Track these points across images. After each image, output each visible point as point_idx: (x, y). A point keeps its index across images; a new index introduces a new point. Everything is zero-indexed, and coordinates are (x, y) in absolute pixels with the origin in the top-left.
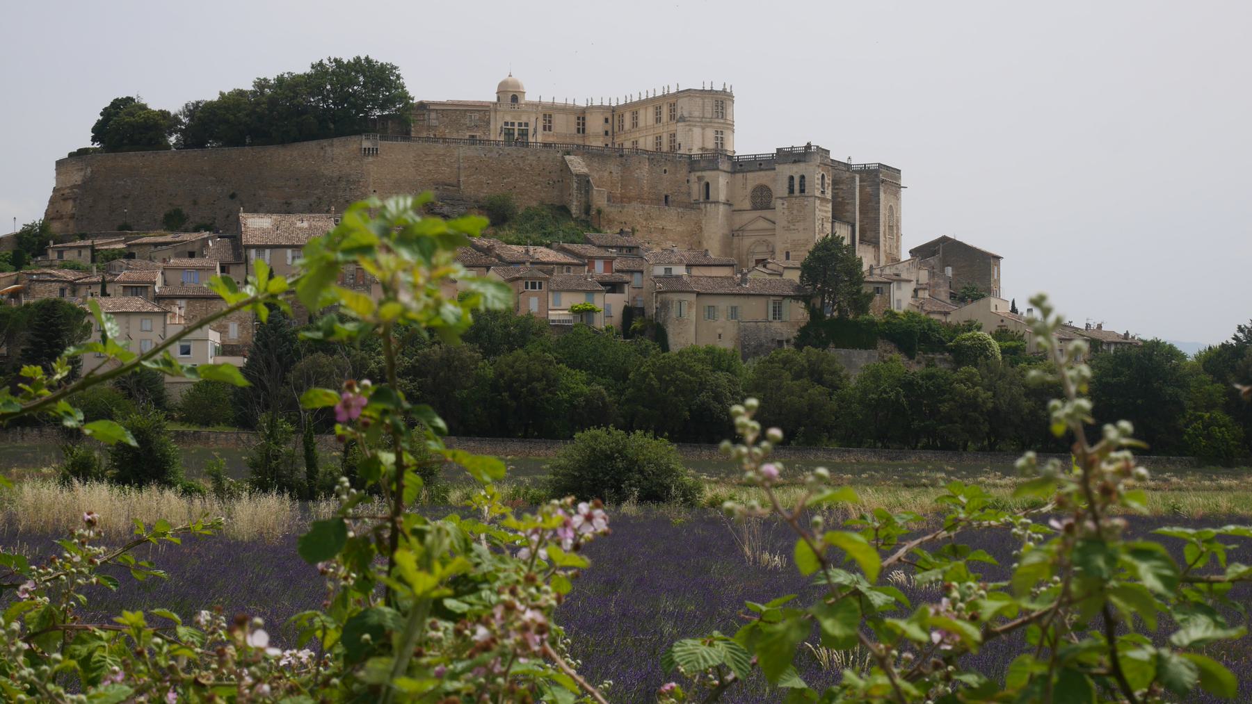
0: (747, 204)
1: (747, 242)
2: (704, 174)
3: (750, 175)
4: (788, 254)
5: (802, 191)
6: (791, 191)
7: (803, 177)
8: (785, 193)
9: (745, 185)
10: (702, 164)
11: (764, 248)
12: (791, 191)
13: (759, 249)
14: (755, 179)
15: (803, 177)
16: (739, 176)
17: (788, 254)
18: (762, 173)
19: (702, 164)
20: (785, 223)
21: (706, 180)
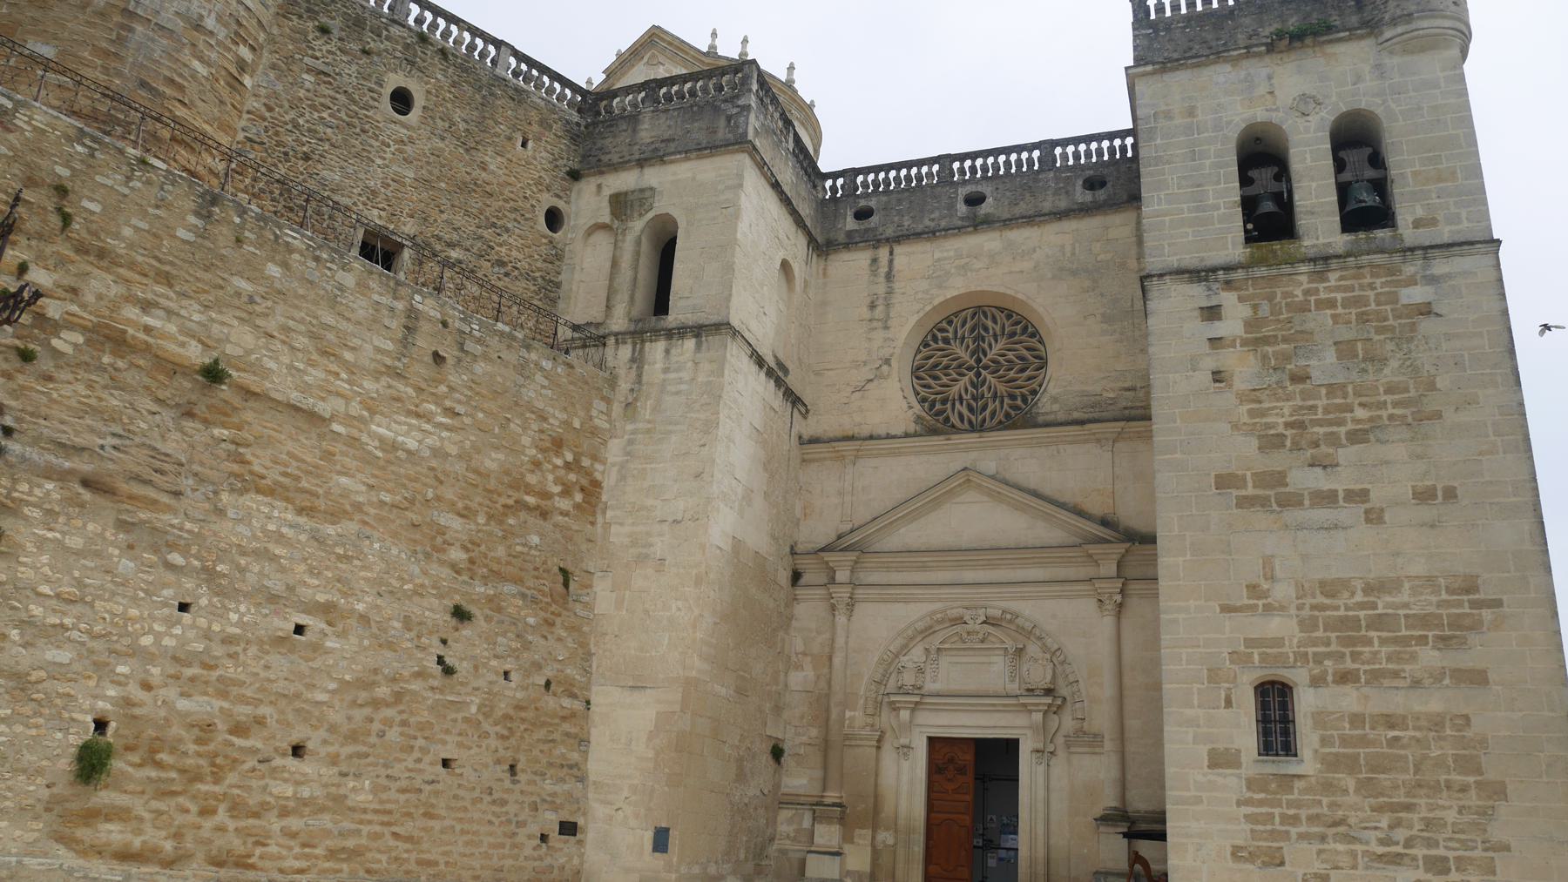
0: (893, 403)
1: (878, 625)
2: (653, 177)
3: (911, 259)
5: (1366, 210)
6: (1270, 221)
8: (1226, 237)
9: (879, 308)
11: (993, 672)
13: (951, 674)
14: (939, 272)
15: (1356, 141)
16: (854, 263)
18: (988, 241)
20: (1243, 453)
21: (661, 206)
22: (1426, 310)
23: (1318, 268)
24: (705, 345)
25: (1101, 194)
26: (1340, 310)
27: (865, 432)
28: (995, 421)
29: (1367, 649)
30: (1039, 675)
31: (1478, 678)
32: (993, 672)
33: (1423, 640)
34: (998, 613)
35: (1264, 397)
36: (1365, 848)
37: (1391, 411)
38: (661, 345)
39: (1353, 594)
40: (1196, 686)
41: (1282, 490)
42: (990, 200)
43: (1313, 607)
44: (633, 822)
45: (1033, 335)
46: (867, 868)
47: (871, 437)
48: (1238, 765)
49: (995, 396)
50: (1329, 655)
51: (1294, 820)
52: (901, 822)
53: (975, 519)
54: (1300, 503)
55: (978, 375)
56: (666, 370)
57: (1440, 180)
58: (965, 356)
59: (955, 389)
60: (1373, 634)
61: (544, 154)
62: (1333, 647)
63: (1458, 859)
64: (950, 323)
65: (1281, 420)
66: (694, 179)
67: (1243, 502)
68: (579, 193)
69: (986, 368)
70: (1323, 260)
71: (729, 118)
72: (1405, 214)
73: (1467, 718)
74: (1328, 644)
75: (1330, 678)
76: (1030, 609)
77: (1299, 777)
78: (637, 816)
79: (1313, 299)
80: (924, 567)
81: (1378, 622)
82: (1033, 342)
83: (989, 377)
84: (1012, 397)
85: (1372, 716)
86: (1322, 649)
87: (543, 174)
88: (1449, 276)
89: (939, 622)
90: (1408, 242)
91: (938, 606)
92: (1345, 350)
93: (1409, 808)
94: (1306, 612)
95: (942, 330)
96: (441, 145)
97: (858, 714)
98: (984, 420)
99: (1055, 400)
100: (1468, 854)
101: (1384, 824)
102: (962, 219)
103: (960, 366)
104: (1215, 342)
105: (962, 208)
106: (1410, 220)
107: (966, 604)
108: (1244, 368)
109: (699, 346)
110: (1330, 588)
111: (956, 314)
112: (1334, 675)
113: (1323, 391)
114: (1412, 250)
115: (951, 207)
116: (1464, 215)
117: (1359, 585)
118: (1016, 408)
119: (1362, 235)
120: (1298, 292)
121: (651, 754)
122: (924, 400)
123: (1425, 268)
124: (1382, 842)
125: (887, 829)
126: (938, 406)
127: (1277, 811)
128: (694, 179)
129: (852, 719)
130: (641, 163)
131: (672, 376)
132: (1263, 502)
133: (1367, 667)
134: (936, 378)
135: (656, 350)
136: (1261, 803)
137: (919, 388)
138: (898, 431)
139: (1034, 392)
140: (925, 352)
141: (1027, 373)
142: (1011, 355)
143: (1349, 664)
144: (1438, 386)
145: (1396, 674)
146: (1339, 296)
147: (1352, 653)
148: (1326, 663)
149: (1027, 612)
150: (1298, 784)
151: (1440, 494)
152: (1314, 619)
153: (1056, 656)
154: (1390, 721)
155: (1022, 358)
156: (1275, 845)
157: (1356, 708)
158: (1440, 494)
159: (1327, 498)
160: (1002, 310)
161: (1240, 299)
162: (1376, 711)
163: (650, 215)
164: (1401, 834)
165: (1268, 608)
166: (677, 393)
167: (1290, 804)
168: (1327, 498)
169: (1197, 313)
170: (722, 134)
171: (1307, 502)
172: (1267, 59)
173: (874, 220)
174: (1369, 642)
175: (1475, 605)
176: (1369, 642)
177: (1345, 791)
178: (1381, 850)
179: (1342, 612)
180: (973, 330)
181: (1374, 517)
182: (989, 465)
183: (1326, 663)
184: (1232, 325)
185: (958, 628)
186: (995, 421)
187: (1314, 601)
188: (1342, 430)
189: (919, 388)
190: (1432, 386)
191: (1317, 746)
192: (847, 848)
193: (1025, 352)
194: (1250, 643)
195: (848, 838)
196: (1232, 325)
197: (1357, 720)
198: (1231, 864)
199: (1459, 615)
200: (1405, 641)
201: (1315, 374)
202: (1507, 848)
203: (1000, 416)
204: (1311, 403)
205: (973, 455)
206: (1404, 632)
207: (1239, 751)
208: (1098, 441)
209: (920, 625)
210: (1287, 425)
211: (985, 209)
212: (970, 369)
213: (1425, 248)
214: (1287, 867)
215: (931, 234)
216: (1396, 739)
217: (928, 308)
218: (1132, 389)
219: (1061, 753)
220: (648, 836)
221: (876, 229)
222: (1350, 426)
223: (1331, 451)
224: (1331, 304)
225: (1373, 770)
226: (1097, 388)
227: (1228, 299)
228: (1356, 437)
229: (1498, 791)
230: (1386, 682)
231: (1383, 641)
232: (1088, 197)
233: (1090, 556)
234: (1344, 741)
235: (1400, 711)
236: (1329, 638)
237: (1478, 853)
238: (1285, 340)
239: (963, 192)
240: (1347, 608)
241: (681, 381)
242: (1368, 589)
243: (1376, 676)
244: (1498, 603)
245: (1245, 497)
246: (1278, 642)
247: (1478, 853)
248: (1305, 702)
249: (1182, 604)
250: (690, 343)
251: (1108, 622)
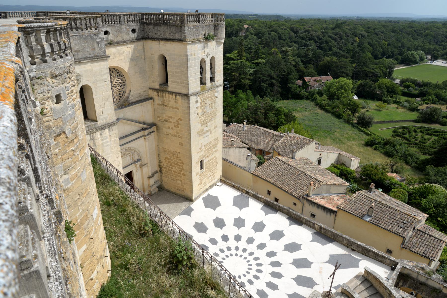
24: (111, 129)
38: (98, 133)
56: (102, 140)
71: (98, 43)
82: (122, 78)
99: (132, 96)
109: (109, 130)
128: (92, 70)
141: (122, 87)
154: (211, 160)
160: (114, 69)
166: (108, 145)
184: (199, 104)
193: (121, 81)
196: (199, 104)
211: (111, 37)
219: (139, 169)
226: (139, 92)
239: (104, 29)
241: (107, 142)
250: (107, 130)
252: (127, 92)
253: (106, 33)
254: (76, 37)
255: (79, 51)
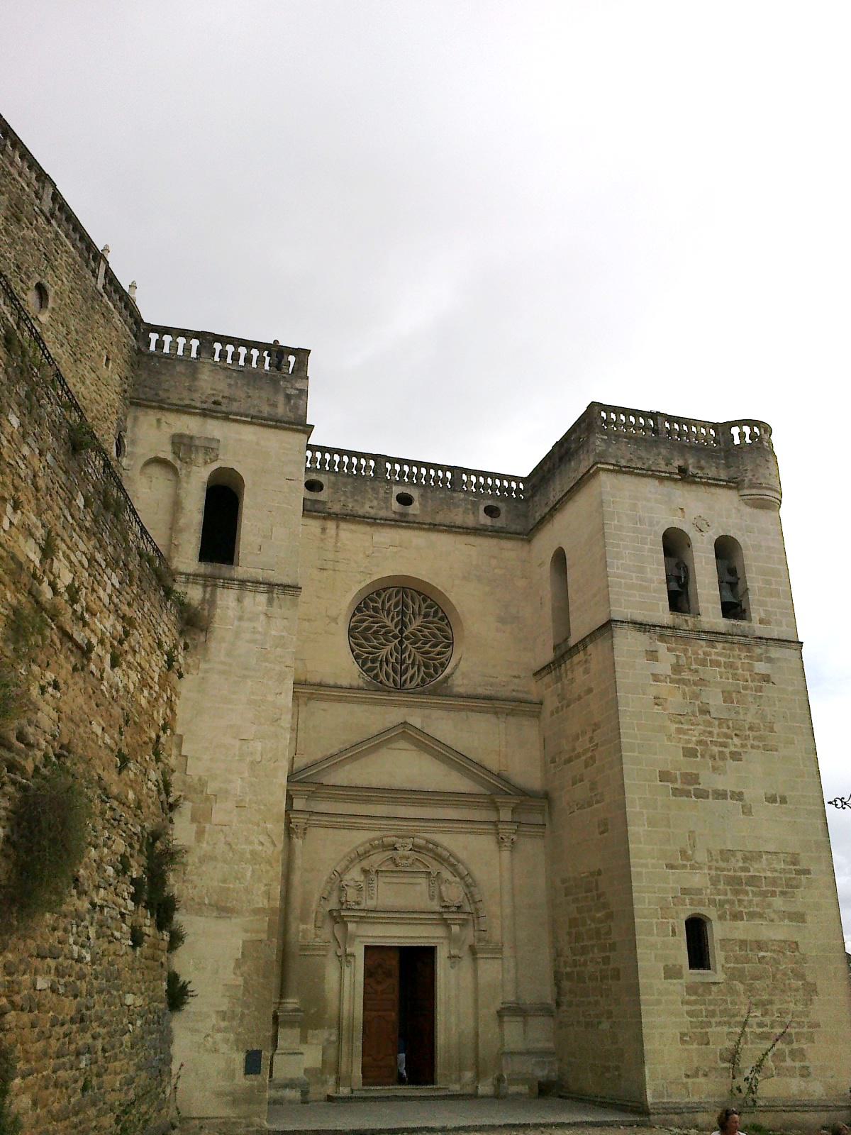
2: (215, 429)
4: (696, 929)
6: (680, 598)
7: (725, 549)
10: (209, 383)
12: (680, 598)
13: (386, 894)
17: (696, 929)
18: (417, 539)
19: (209, 383)
21: (227, 460)
22: (766, 678)
23: (713, 638)
24: (276, 602)
25: (500, 522)
26: (723, 669)
27: (316, 679)
28: (414, 683)
29: (746, 898)
30: (454, 893)
31: (799, 917)
32: (416, 894)
33: (773, 894)
34: (422, 842)
35: (683, 721)
36: (751, 1030)
37: (752, 742)
39: (738, 861)
40: (655, 920)
41: (697, 786)
42: (416, 504)
43: (717, 869)
44: (224, 1048)
45: (442, 619)
46: (319, 1065)
47: (320, 685)
48: (681, 978)
49: (413, 664)
50: (728, 901)
51: (713, 1014)
52: (345, 1023)
53: (404, 767)
54: (708, 797)
55: (401, 643)
56: (240, 619)
57: (771, 595)
58: (392, 626)
59: (383, 653)
60: (749, 888)
61: (117, 378)
62: (730, 896)
63: (796, 1033)
64: (379, 595)
65: (694, 739)
66: (258, 444)
67: (676, 792)
68: (136, 419)
69: (407, 638)
70: (713, 636)
71: (288, 397)
72: (756, 612)
73: (796, 943)
74: (726, 895)
75: (728, 917)
76: (451, 842)
77: (714, 983)
78: (227, 1041)
79: (708, 658)
80: (367, 801)
81: (753, 880)
83: (410, 646)
84: (427, 666)
85: (751, 941)
86: (722, 897)
87: (115, 396)
88: (778, 659)
89: (374, 847)
90: (758, 634)
91: (378, 834)
92: (727, 698)
93: (771, 1002)
94: (713, 872)
95: (373, 600)
96: (60, 351)
97: (310, 927)
98: (405, 681)
100: (801, 1030)
101: (758, 1014)
102: (395, 512)
103: (386, 633)
104: (656, 678)
105: (395, 505)
106: (758, 618)
107: (400, 833)
108: (675, 698)
109: (270, 602)
110: (726, 855)
111: (385, 590)
112: (730, 913)
113: (716, 723)
114: (760, 638)
115: (387, 500)
116: (784, 623)
117: (739, 855)
118: (431, 676)
119: (733, 622)
120: (700, 652)
121: (240, 981)
122: (357, 657)
123: (767, 651)
124: (760, 1025)
125: (330, 1027)
126: (369, 664)
127: (703, 1007)
128: (258, 444)
129: (305, 932)
130: (205, 414)
131: (246, 624)
132: (687, 794)
133: (746, 911)
134: (367, 639)
135: (227, 600)
136: (695, 1002)
137: (352, 644)
138: (345, 683)
139: (443, 666)
140: (359, 616)
141: (438, 649)
142: (426, 632)
143: (737, 908)
144: (775, 730)
145: (761, 916)
146: (722, 659)
147: (739, 900)
148: (727, 906)
149: (445, 844)
150: (714, 988)
151: (778, 799)
152: (718, 876)
153: (469, 884)
154: (760, 945)
155: (434, 635)
156: (703, 1031)
157: (742, 937)
158: (778, 799)
159: (721, 795)
160: (419, 593)
161: (669, 649)
162: (753, 939)
163: (215, 466)
164: (767, 1020)
165: (692, 867)
167: (711, 1003)
168: (721, 795)
169: (644, 654)
170: (281, 410)
171: (711, 797)
172: (680, 484)
173: (323, 496)
174: (746, 893)
175: (799, 872)
176: (746, 893)
177: (738, 995)
178: (759, 1030)
179: (731, 873)
180: (396, 605)
181: (747, 811)
182: (416, 719)
183: (727, 906)
184: (664, 666)
185: (389, 854)
186: (414, 683)
187: (717, 865)
188: (727, 750)
189: (352, 644)
190: (772, 730)
191: (723, 962)
192: (303, 1048)
193: (436, 631)
194: (685, 891)
195: (304, 1040)
197: (743, 944)
198: (680, 1046)
199: (790, 878)
200: (764, 894)
201: (712, 710)
202: (818, 1025)
203: (417, 680)
204: (709, 729)
205: (404, 710)
206: (765, 889)
207: (681, 966)
208: (496, 713)
209: (361, 850)
210: (700, 742)
211: (414, 509)
212: (395, 637)
213: (767, 639)
214: (711, 1046)
215: (372, 521)
216: (763, 957)
217: (369, 581)
218: (519, 677)
220: (239, 1059)
221: (324, 503)
222: (733, 749)
223: (721, 763)
224: (718, 664)
225: (752, 979)
227: (662, 647)
228: (736, 756)
229: (811, 989)
230: (758, 921)
231: (755, 894)
232: (485, 520)
233: (495, 803)
234: (737, 960)
235: (765, 939)
236: (726, 890)
237: (805, 1030)
238: (695, 684)
239: (397, 490)
240: (735, 871)
241: (254, 631)
242: (745, 859)
243: (752, 915)
244: (807, 872)
245: (677, 789)
246: (699, 891)
247: (805, 1030)
248: (717, 932)
249: (642, 861)
250: (262, 598)
251: (506, 854)
252: (452, 664)
253: (405, 500)
254: (235, 374)
255: (235, 400)
